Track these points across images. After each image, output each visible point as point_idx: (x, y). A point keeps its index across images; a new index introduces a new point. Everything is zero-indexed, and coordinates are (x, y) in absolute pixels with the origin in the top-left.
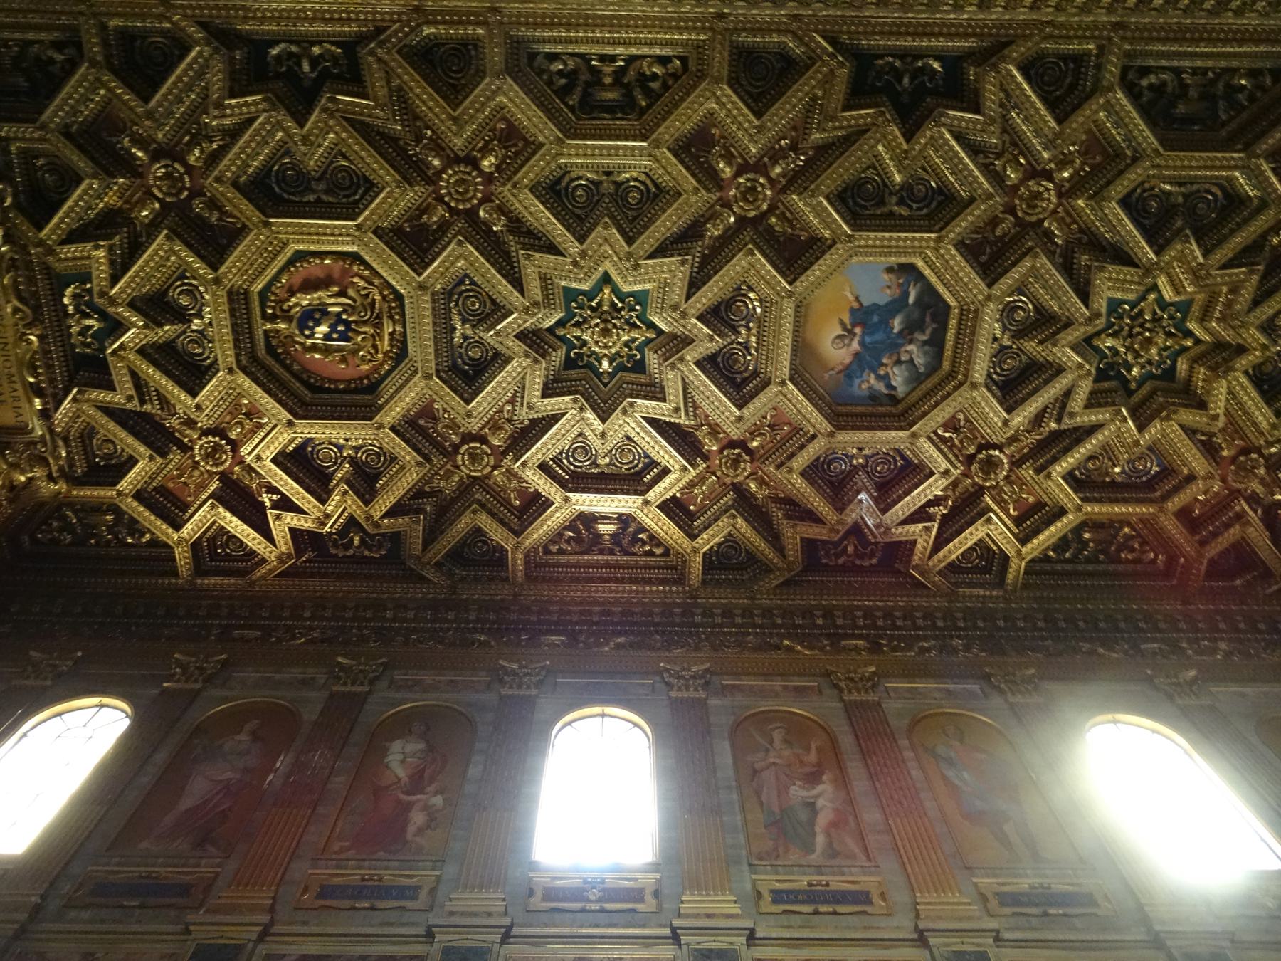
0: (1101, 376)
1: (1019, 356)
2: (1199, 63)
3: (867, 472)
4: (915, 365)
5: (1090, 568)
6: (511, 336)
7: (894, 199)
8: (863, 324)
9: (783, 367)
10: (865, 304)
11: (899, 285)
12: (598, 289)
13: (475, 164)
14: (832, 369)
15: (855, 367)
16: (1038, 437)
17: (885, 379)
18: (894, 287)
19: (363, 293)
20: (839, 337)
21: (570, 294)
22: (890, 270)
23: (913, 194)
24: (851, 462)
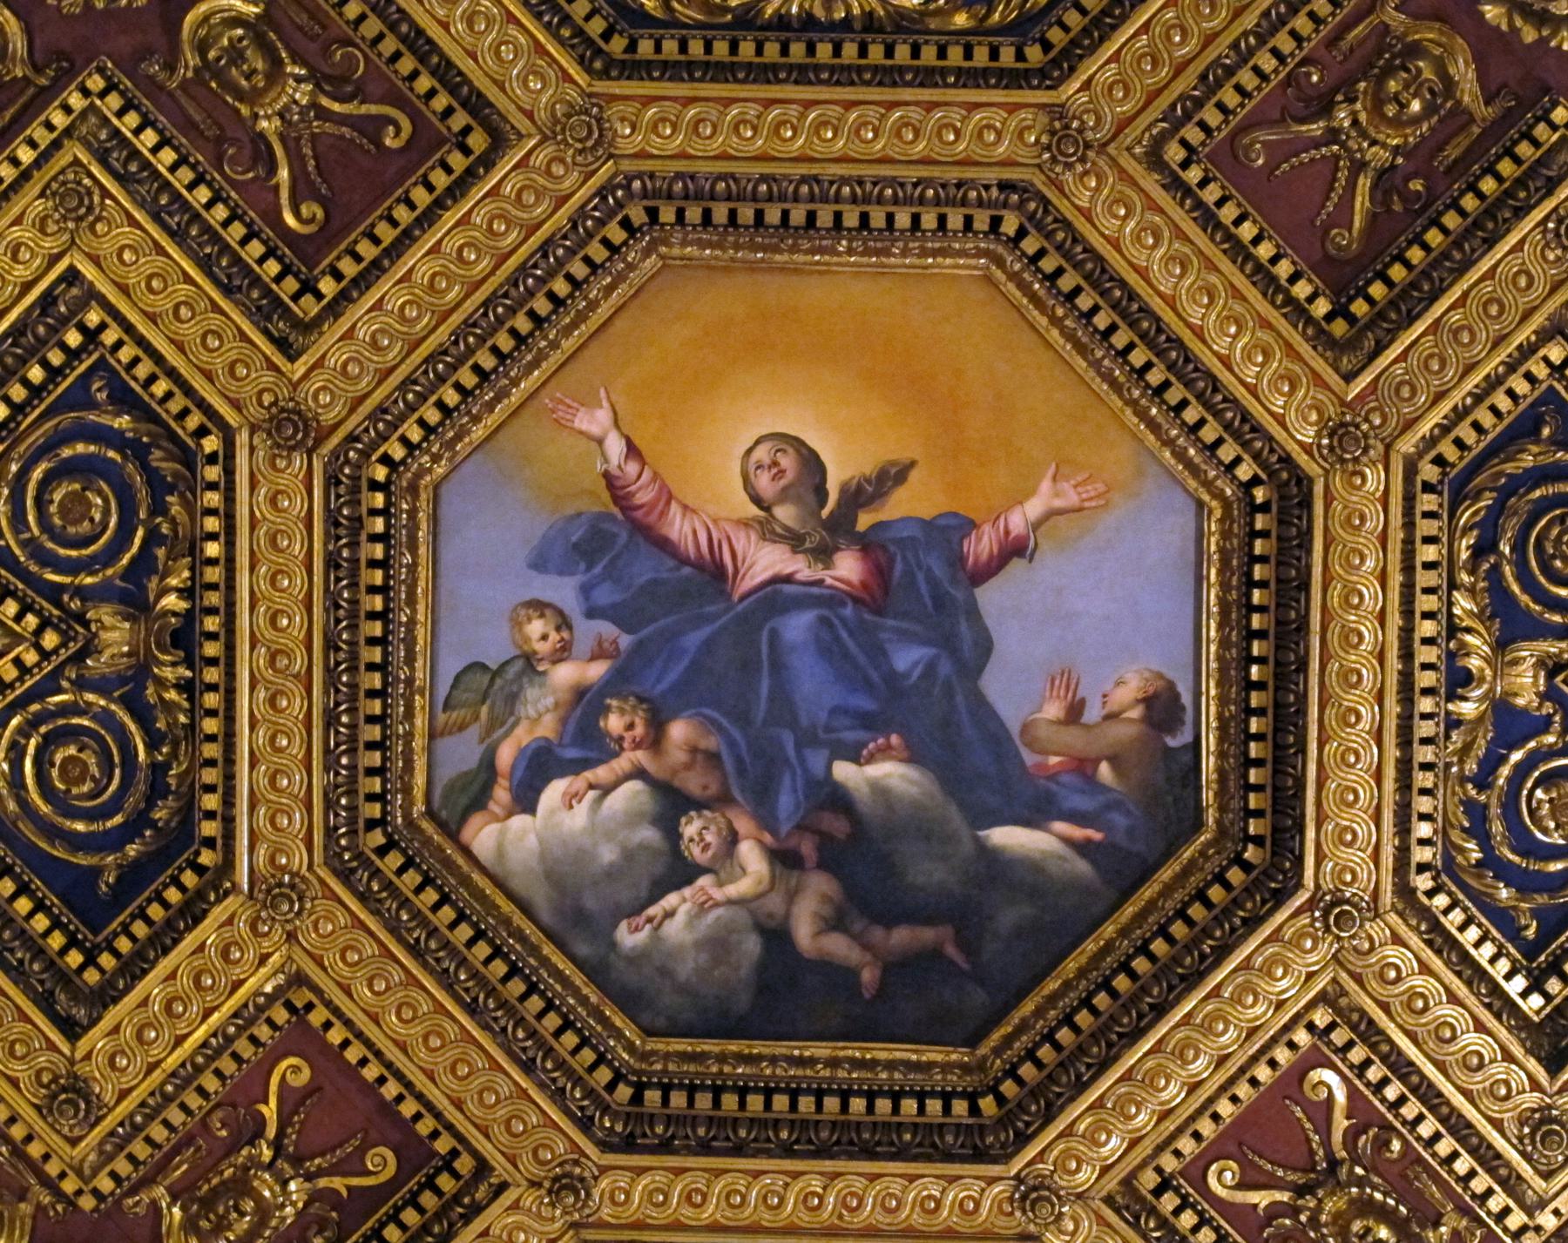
3: (51, 685)
4: (659, 889)
10: (990, 597)
11: (1083, 767)
14: (632, 450)
15: (646, 568)
18: (1072, 738)
20: (812, 464)
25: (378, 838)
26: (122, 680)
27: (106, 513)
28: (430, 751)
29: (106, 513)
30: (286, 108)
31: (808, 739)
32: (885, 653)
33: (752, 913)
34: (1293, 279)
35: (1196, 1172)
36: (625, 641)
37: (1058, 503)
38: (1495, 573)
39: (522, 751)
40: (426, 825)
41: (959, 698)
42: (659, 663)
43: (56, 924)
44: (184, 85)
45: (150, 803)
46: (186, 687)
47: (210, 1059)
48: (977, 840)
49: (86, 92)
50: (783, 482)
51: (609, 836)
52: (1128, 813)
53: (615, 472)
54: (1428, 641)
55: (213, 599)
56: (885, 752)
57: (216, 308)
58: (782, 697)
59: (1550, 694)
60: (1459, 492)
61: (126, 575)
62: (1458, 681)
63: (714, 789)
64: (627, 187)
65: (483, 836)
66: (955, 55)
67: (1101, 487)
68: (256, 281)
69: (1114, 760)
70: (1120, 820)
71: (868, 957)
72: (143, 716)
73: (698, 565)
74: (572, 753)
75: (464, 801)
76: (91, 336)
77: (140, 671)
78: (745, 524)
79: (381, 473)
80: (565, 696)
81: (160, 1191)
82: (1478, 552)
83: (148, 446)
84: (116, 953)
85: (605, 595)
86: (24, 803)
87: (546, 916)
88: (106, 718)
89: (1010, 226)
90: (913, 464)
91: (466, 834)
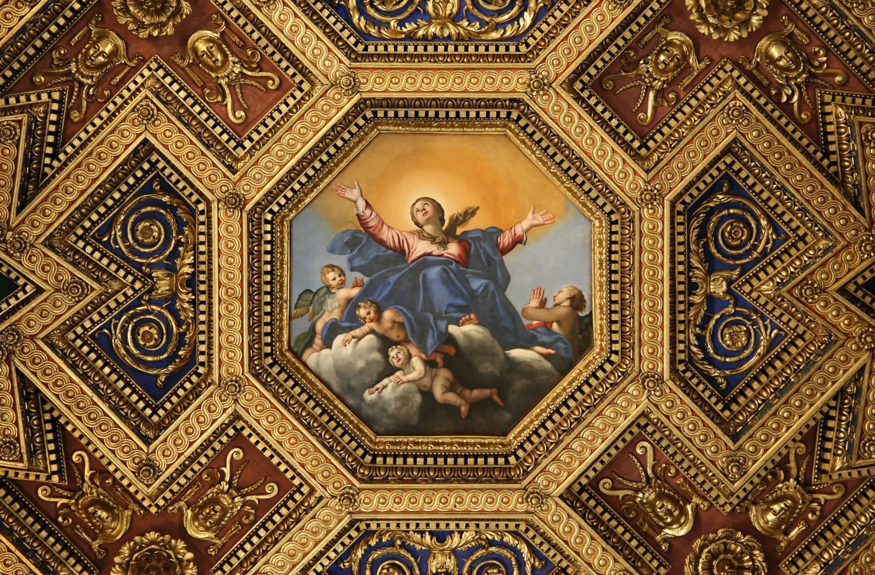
7: (718, 288)
8: (464, 260)
10: (508, 259)
14: (368, 205)
15: (374, 251)
18: (542, 313)
20: (439, 209)
23: (729, 325)
25: (269, 360)
26: (166, 299)
27: (160, 234)
28: (289, 325)
29: (160, 234)
30: (230, 74)
31: (438, 317)
32: (468, 282)
33: (418, 386)
34: (625, 133)
35: (594, 483)
36: (366, 280)
37: (535, 222)
38: (706, 246)
39: (326, 324)
40: (288, 354)
41: (498, 299)
42: (380, 288)
43: (141, 398)
44: (189, 65)
45: (179, 349)
46: (193, 302)
47: (203, 450)
48: (506, 355)
49: (150, 69)
50: (427, 216)
51: (361, 357)
52: (565, 343)
53: (361, 214)
54: (680, 273)
55: (203, 267)
56: (469, 321)
57: (203, 154)
58: (428, 300)
59: (729, 292)
60: (690, 213)
61: (168, 258)
62: (692, 288)
63: (402, 336)
64: (365, 104)
65: (311, 358)
66: (492, 49)
67: (551, 216)
68: (219, 142)
69: (558, 322)
70: (561, 345)
71: (463, 402)
72: (175, 313)
73: (394, 249)
74: (346, 324)
75: (303, 344)
76: (153, 165)
77: (173, 296)
78: (412, 233)
79: (269, 217)
80: (343, 302)
81: (182, 503)
82: (700, 237)
83: (177, 207)
84: (165, 409)
85: (358, 262)
86: (127, 350)
87: (336, 389)
88: (160, 315)
89: (514, 116)
90: (478, 208)
91: (305, 357)
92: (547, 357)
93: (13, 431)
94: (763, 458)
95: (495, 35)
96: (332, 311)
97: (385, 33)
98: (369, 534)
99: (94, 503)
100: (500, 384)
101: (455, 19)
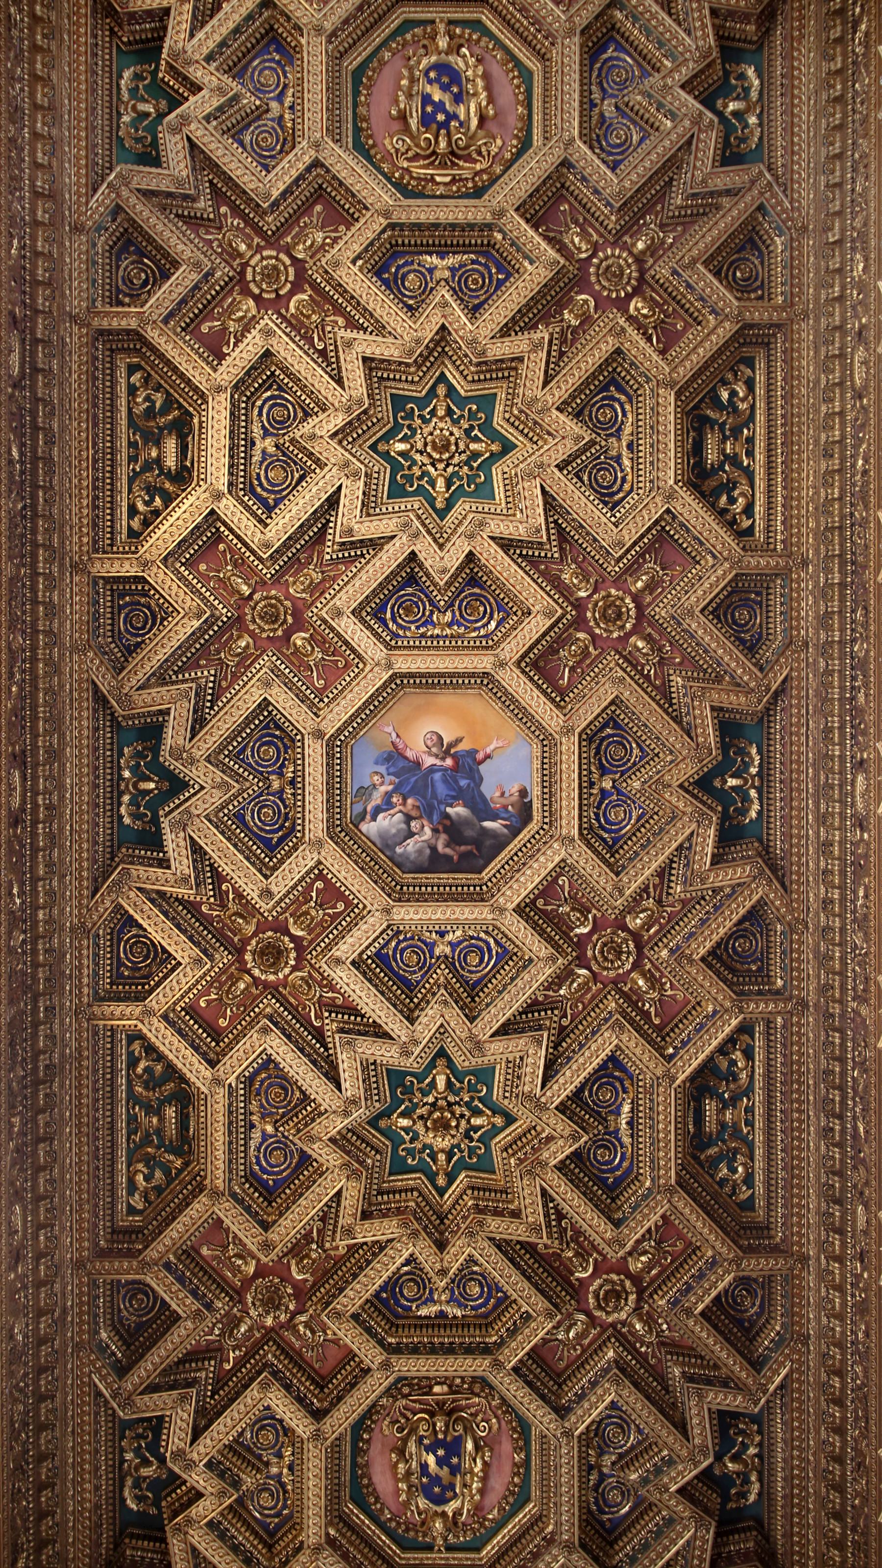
0: (396, 1077)
1: (421, 969)
2: (759, 1111)
3: (261, 795)
5: (122, 1124)
6: (443, 320)
7: (607, 784)
8: (456, 768)
9: (405, 663)
10: (482, 768)
12: (494, 435)
13: (637, 291)
15: (401, 764)
16: (312, 1014)
17: (387, 805)
18: (503, 801)
19: (483, 149)
20: (440, 738)
21: (487, 402)
22: (523, 793)
24: (273, 772)
31: (440, 802)
35: (533, 902)
38: (600, 760)
46: (293, 794)
59: (614, 787)
60: (590, 740)
62: (592, 784)
72: (283, 801)
77: (282, 791)
85: (392, 770)
92: (505, 826)
93: (187, 871)
94: (634, 886)
95: (474, 634)
96: (376, 799)
97: (408, 634)
98: (399, 932)
99: (235, 914)
100: (477, 842)
101: (450, 625)
